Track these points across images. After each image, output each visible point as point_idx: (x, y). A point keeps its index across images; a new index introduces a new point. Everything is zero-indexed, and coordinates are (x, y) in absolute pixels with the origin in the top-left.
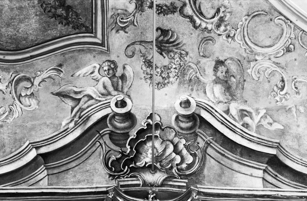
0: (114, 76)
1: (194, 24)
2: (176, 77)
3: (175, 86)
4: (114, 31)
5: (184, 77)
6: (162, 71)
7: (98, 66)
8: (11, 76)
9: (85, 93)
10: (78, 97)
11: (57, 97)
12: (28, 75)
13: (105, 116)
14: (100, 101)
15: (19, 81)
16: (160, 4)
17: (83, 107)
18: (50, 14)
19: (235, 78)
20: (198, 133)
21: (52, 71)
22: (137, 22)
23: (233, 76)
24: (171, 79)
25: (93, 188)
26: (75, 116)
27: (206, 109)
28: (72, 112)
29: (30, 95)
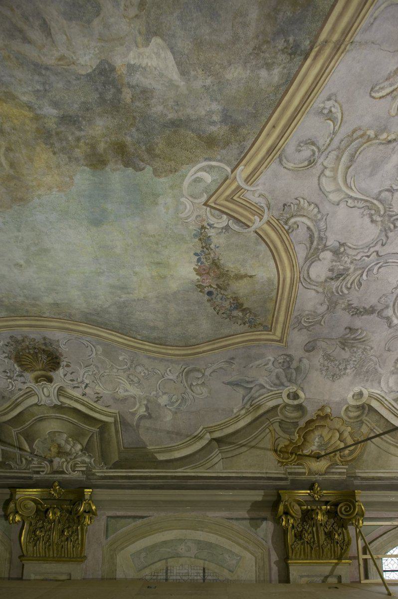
0: (289, 367)
1: (390, 324)
7: (272, 359)
11: (229, 386)
12: (198, 367)
13: (276, 406)
14: (272, 391)
16: (357, 307)
17: (254, 396)
18: (225, 316)
20: (365, 421)
22: (325, 322)
24: (348, 371)
25: (263, 473)
26: (246, 404)
27: (377, 400)
28: (243, 400)
29: (202, 384)
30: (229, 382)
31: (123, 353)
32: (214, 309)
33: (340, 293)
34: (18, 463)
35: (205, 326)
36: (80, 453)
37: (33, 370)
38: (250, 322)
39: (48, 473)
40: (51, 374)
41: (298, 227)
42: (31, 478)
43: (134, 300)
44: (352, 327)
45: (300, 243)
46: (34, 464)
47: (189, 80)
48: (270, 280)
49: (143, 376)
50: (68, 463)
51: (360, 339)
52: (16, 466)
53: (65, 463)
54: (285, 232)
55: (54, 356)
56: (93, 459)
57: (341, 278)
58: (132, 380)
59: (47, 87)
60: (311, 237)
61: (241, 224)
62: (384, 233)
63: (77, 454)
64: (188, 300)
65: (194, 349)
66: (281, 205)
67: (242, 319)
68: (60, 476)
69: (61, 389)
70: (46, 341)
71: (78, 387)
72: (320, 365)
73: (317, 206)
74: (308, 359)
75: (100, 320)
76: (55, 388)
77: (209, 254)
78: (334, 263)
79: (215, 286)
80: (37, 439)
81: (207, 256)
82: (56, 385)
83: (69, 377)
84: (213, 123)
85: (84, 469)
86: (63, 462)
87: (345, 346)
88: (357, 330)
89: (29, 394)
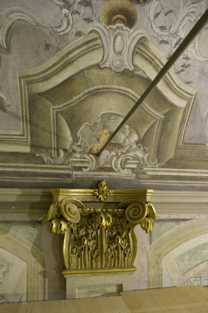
34: (53, 156)
36: (134, 146)
39: (93, 169)
40: (137, 8)
42: (69, 176)
46: (75, 157)
50: (118, 158)
52: (50, 159)
53: (115, 158)
56: (147, 155)
63: (131, 147)
68: (107, 173)
69: (142, 42)
71: (166, 42)
76: (134, 38)
80: (85, 122)
82: (136, 32)
83: (161, 20)
85: (135, 166)
86: (113, 156)
89: (91, 44)
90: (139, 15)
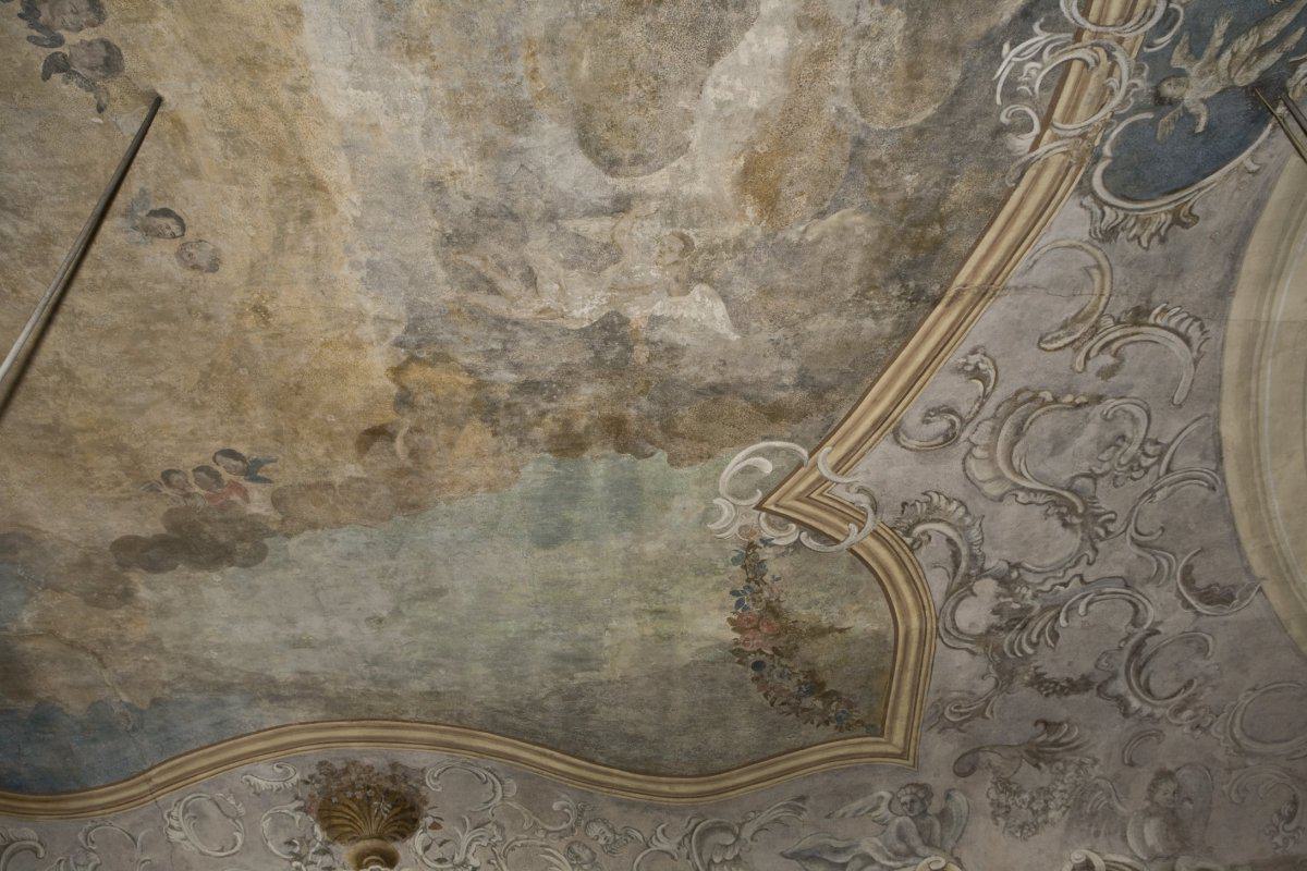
0: (924, 813)
1: (1126, 709)
2: (1064, 809)
3: (1059, 831)
4: (935, 730)
5: (1080, 807)
6: (1033, 799)
7: (887, 796)
8: (689, 822)
9: (857, 851)
10: (841, 860)
11: (794, 861)
15: (709, 830)
18: (786, 708)
19: (1192, 803)
21: (782, 810)
23: (1189, 799)
24: (1052, 814)
30: (795, 853)
31: (564, 796)
32: (766, 695)
33: (1020, 655)
35: (746, 732)
37: (355, 838)
38: (839, 719)
40: (395, 846)
41: (930, 538)
43: (601, 683)
44: (1048, 718)
45: (935, 567)
47: (748, 333)
48: (878, 637)
49: (602, 846)
51: (1068, 743)
54: (905, 548)
55: (408, 805)
57: (1018, 626)
58: (578, 857)
59: (509, 346)
60: (956, 555)
61: (824, 538)
62: (1088, 544)
64: (713, 680)
65: (718, 780)
66: (898, 505)
67: (823, 713)
70: (398, 772)
72: (992, 804)
73: (962, 503)
74: (965, 793)
75: (521, 724)
77: (761, 591)
78: (1002, 600)
79: (769, 652)
81: (756, 596)
83: (437, 852)
84: (783, 387)
87: (1039, 759)
88: (1060, 724)
90: (401, 853)
